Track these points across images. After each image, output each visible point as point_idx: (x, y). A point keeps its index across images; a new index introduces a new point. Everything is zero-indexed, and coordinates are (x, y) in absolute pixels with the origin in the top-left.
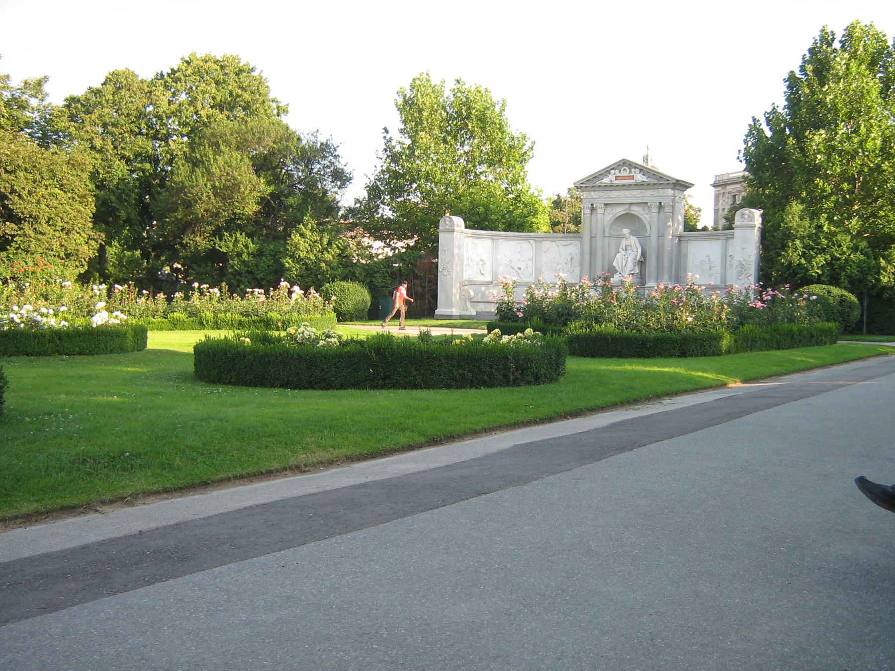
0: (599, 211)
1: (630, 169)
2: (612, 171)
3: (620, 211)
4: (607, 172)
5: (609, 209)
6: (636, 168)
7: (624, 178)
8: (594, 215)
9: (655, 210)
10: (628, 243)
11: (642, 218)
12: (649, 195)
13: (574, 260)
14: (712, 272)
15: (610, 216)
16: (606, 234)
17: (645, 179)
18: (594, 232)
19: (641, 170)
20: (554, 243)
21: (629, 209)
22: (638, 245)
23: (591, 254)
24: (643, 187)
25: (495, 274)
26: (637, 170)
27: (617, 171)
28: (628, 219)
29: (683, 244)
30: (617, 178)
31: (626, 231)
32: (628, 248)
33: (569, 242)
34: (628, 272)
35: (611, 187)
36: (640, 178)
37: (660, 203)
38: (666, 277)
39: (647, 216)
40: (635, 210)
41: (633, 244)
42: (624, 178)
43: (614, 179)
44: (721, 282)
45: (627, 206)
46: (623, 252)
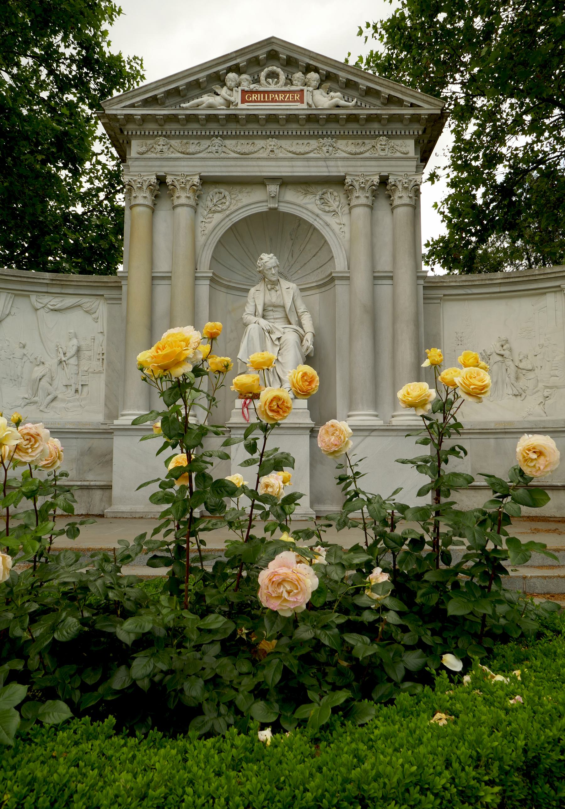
0: (183, 197)
3: (251, 202)
4: (211, 77)
5: (212, 196)
6: (308, 69)
13: (85, 354)
14: (522, 383)
17: (337, 97)
18: (163, 266)
20: (22, 304)
24: (333, 128)
26: (313, 76)
27: (244, 76)
31: (268, 259)
32: (271, 314)
33: (70, 301)
35: (231, 124)
36: (324, 100)
39: (332, 221)
40: (299, 203)
41: (288, 304)
43: (236, 97)
45: (273, 188)
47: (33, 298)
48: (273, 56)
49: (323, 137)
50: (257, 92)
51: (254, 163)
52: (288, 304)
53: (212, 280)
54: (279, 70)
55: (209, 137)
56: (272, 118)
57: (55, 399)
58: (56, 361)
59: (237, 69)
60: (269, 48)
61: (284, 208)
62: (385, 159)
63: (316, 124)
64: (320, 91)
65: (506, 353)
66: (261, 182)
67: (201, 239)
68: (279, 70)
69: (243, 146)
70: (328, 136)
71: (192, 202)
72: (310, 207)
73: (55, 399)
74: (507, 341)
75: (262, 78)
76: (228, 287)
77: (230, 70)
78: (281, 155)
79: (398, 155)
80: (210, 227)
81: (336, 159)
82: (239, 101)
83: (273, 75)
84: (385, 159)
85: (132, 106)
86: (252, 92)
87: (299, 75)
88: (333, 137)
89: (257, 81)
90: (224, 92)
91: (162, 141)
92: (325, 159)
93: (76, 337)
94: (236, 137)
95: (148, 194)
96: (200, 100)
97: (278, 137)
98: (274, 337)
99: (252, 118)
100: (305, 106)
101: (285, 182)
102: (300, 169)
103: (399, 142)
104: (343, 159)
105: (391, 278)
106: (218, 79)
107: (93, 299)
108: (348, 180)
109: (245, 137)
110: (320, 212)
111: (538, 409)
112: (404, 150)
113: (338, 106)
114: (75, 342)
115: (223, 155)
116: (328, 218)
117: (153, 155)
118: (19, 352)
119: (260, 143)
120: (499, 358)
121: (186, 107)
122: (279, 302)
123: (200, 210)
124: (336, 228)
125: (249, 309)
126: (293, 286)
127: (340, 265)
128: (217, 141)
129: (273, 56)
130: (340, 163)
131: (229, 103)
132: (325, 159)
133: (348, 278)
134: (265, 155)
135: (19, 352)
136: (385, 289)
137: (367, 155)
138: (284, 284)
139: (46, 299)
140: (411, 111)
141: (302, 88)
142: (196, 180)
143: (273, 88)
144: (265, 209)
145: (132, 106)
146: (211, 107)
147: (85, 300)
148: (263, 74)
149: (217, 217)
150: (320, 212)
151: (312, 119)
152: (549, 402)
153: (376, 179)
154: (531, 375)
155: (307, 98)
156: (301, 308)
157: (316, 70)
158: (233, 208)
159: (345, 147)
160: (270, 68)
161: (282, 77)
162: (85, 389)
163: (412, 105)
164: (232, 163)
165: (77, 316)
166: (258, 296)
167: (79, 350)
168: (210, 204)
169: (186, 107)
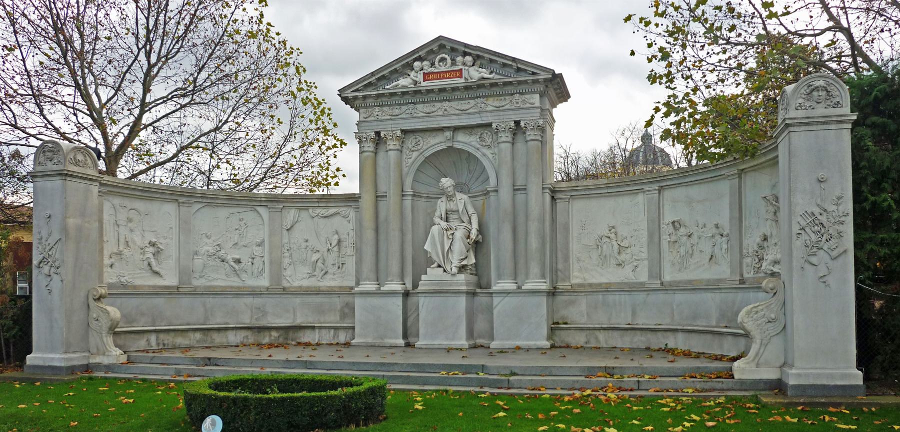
0: (392, 144)
1: (453, 60)
2: (417, 64)
3: (436, 143)
4: (404, 65)
5: (410, 142)
6: (465, 54)
7: (440, 75)
8: (381, 155)
9: (506, 137)
10: (452, 206)
11: (478, 155)
12: (488, 110)
13: (344, 244)
14: (623, 257)
15: (415, 154)
16: (408, 189)
18: (382, 188)
19: (477, 58)
20: (304, 214)
21: (452, 139)
22: (471, 210)
23: (377, 230)
25: (185, 273)
26: (469, 59)
27: (425, 63)
28: (450, 159)
29: (560, 205)
30: (426, 77)
31: (446, 182)
32: (452, 217)
33: (333, 211)
34: (456, 263)
37: (517, 123)
38: (535, 269)
39: (488, 152)
41: (461, 208)
42: (440, 75)
43: (420, 77)
44: (651, 276)
45: (449, 134)
46: (444, 224)
47: (310, 210)
48: (442, 47)
49: (477, 97)
50: (433, 73)
51: (434, 119)
52: (461, 208)
53: (413, 195)
54: (446, 56)
55: (407, 104)
56: (442, 90)
57: (326, 273)
58: (326, 249)
59: (420, 59)
60: (439, 43)
61: (457, 146)
62: (518, 109)
63: (473, 89)
64: (475, 67)
65: (612, 236)
66: (441, 130)
67: (405, 169)
68: (446, 56)
69: (427, 108)
70: (480, 97)
71: (398, 147)
72: (473, 143)
73: (326, 273)
74: (613, 227)
75: (436, 63)
76: (427, 197)
77: (415, 60)
78: (452, 112)
79: (528, 105)
80: (411, 161)
81: (487, 112)
82: (422, 80)
83: (443, 60)
84: (518, 109)
85: (357, 90)
86: (429, 73)
87: (459, 59)
88: (483, 97)
89: (433, 64)
90: (412, 74)
91: (377, 109)
92: (479, 112)
93: (337, 233)
94: (423, 102)
95: (371, 144)
96: (395, 83)
97: (449, 101)
98: (449, 233)
99: (429, 91)
100: (463, 80)
101: (456, 129)
102: (464, 122)
103: (527, 96)
104: (491, 111)
105: (525, 189)
106: (410, 66)
107: (346, 208)
108: (494, 126)
109: (428, 102)
110: (479, 146)
111: (631, 275)
112: (532, 101)
113: (483, 78)
114: (336, 237)
115: (415, 115)
116: (485, 150)
117: (373, 119)
118: (304, 245)
119: (438, 105)
120: (607, 240)
121: (389, 87)
122: (454, 209)
123: (404, 150)
124: (491, 156)
125: (437, 214)
126: (465, 197)
127: (493, 182)
128: (411, 106)
129: (442, 47)
130: (489, 114)
131: (415, 83)
132: (479, 112)
133: (497, 191)
134: (440, 113)
135: (304, 245)
136: (520, 197)
137: (506, 107)
138: (459, 196)
139: (318, 211)
140: (531, 78)
141: (461, 67)
142: (399, 133)
143: (443, 69)
144: (444, 147)
145: (357, 90)
146: (403, 87)
147: (342, 209)
148: (437, 60)
149: (415, 154)
150: (479, 146)
151: (467, 88)
152: (638, 269)
153: (512, 124)
154: (629, 251)
155: (465, 74)
156: (471, 210)
157: (470, 54)
158: (425, 148)
159: (492, 103)
160: (441, 56)
161: (449, 61)
162: (345, 266)
163: (533, 73)
164: (421, 120)
165: (337, 219)
166: (442, 206)
167: (339, 241)
168: (411, 147)
169: (389, 87)
